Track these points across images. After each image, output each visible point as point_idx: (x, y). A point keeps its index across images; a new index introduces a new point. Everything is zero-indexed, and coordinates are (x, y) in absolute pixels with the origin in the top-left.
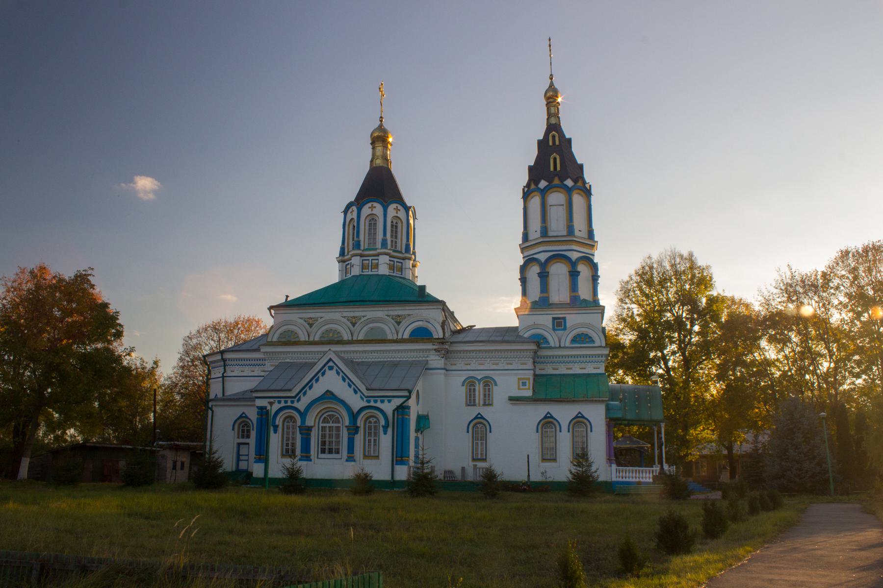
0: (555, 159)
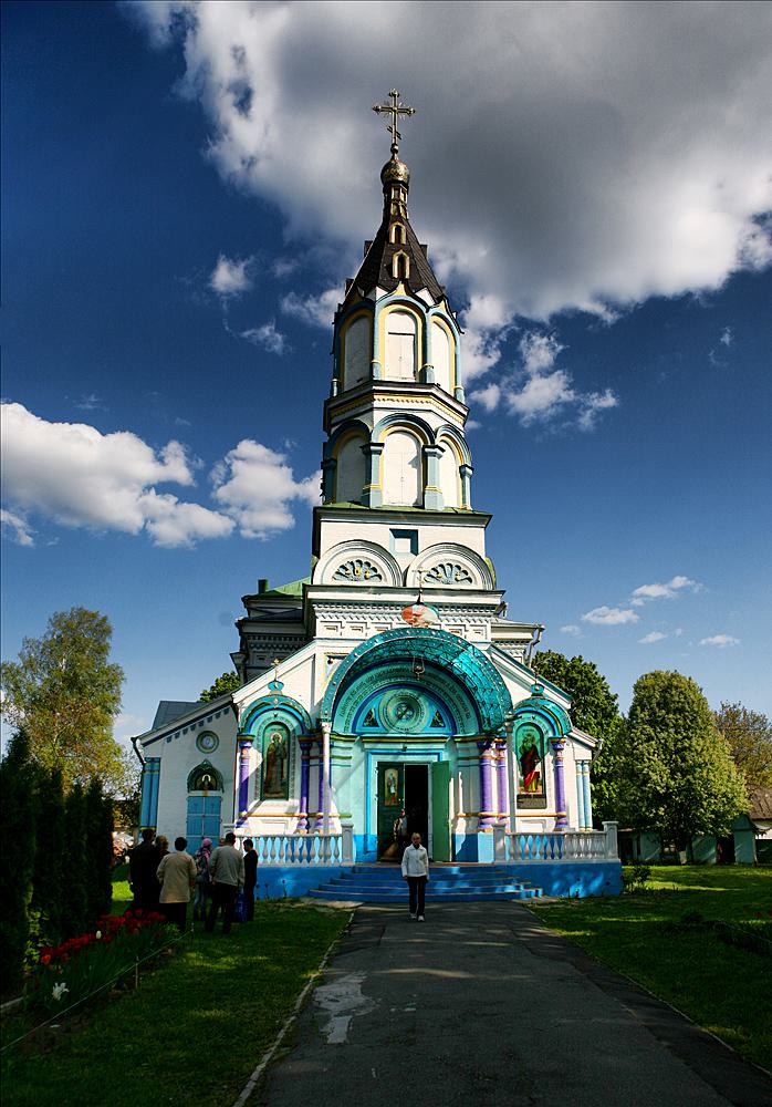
0: (402, 260)
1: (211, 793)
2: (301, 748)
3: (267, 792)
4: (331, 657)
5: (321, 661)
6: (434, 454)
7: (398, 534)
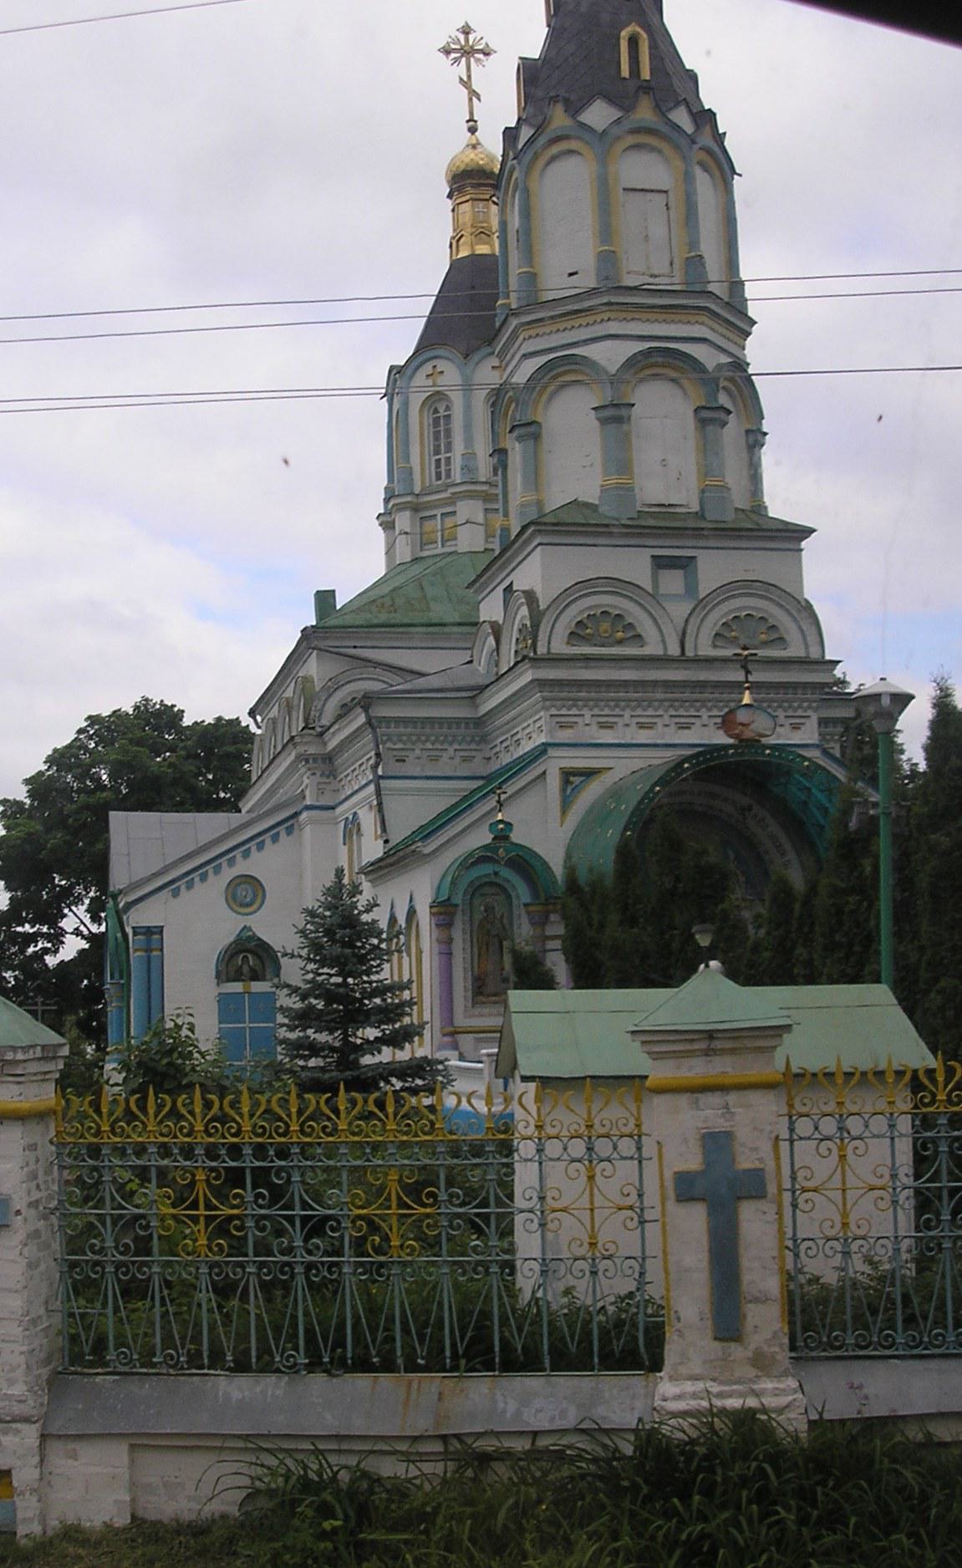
0: (633, 41)
1: (258, 987)
2: (533, 924)
3: (481, 994)
4: (567, 775)
5: (554, 781)
6: (712, 421)
7: (660, 563)
